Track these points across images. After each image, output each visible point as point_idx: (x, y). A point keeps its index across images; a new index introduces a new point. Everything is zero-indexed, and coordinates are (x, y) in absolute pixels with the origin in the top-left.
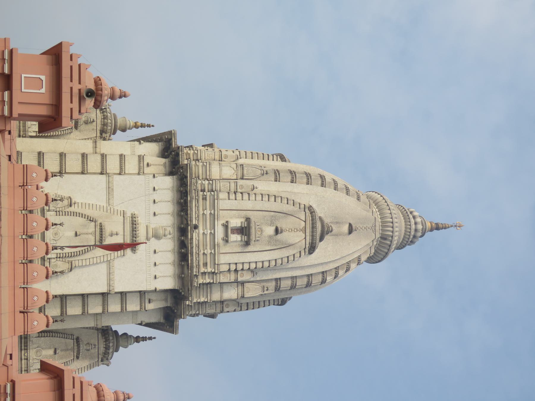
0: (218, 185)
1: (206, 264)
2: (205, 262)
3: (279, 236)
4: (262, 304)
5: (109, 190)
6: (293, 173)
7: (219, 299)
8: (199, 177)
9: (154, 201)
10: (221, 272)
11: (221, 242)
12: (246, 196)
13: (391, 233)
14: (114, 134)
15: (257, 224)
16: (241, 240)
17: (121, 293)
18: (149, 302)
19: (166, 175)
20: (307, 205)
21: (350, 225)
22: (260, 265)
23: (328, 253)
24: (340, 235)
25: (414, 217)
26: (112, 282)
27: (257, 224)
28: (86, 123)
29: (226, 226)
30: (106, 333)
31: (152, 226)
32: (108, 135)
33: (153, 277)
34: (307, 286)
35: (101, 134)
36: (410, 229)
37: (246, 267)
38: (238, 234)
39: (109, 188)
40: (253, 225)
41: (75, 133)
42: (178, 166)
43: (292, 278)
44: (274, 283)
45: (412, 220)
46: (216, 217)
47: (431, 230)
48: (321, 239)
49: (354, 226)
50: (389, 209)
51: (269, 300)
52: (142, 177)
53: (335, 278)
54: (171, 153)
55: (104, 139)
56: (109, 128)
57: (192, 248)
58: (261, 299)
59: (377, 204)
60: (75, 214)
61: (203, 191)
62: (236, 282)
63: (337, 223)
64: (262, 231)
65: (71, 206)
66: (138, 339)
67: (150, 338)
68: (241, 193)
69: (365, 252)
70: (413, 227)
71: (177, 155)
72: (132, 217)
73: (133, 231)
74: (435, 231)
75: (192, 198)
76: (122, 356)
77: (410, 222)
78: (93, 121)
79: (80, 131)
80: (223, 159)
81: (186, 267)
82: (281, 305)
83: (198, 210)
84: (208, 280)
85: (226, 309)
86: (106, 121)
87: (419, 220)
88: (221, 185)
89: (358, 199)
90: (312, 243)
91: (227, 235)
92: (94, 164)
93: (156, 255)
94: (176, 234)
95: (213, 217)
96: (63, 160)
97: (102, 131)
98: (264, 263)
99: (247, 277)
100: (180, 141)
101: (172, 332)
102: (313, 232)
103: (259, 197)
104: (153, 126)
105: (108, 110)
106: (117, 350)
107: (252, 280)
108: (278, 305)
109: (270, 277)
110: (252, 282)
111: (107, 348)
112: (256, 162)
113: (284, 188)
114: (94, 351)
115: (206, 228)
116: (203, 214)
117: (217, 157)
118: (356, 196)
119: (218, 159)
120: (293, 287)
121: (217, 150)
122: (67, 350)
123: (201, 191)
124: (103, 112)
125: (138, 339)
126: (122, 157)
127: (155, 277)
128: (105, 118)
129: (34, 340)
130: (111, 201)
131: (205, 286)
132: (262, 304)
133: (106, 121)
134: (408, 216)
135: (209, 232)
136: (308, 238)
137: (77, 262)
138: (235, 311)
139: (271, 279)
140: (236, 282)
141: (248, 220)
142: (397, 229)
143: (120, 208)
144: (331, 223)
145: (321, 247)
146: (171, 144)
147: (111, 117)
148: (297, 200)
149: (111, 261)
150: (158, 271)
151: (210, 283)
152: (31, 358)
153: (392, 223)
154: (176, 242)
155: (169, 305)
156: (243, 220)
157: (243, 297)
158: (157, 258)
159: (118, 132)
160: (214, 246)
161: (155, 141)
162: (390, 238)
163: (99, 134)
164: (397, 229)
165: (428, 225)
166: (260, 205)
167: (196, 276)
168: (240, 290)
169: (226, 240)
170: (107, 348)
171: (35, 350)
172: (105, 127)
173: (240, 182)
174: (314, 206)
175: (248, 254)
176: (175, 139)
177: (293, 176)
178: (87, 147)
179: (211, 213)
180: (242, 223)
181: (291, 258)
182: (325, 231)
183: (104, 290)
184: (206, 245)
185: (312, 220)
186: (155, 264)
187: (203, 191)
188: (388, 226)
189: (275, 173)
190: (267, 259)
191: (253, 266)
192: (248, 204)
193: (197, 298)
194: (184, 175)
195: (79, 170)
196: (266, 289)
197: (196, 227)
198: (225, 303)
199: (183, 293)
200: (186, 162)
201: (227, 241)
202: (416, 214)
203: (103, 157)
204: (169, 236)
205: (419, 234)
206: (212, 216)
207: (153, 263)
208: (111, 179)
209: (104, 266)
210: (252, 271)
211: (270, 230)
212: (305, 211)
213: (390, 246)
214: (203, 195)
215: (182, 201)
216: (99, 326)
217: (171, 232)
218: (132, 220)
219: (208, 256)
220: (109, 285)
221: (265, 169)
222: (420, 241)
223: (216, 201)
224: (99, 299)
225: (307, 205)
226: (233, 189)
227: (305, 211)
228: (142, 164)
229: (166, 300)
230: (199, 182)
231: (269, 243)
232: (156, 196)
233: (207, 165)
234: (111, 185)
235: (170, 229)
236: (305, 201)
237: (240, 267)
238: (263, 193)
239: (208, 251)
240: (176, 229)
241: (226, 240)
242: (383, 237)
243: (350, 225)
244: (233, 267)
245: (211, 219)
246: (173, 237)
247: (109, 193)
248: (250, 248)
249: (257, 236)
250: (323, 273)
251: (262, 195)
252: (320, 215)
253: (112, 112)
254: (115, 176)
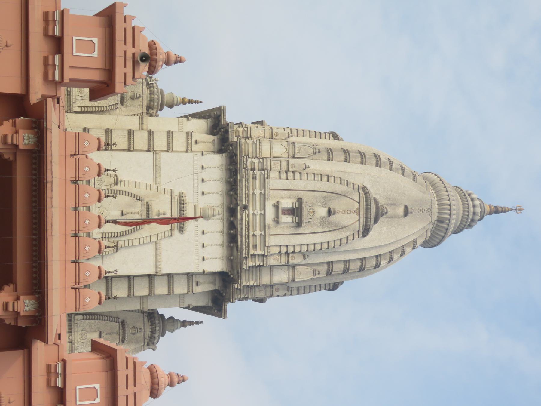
0: (269, 164)
1: (256, 245)
2: (255, 243)
3: (332, 218)
4: (313, 288)
5: (157, 167)
6: (346, 152)
7: (269, 283)
8: (248, 155)
9: (203, 180)
10: (271, 255)
11: (272, 223)
12: (297, 176)
13: (448, 216)
14: (161, 110)
15: (309, 205)
16: (293, 222)
17: (168, 275)
18: (197, 285)
19: (214, 152)
20: (361, 186)
21: (406, 207)
22: (311, 248)
23: (382, 235)
24: (396, 217)
25: (472, 200)
26: (158, 264)
27: (309, 205)
28: (132, 98)
29: (277, 206)
30: (152, 316)
31: (201, 206)
32: (155, 111)
33: (201, 259)
34: (360, 271)
35: (148, 110)
36: (468, 212)
37: (297, 249)
38: (289, 215)
39: (156, 165)
40: (304, 206)
41: (121, 109)
42: (227, 143)
43: (345, 261)
44: (325, 267)
45: (471, 203)
46: (266, 197)
47: (490, 214)
48: (376, 221)
49: (409, 208)
50: (447, 191)
51: (321, 285)
52: (190, 155)
53: (389, 262)
54: (220, 129)
55: (151, 115)
56: (156, 104)
57: (242, 229)
58: (312, 284)
59: (433, 185)
60: (122, 193)
61: (253, 169)
62: (287, 265)
63: (392, 204)
64: (314, 212)
65: (117, 184)
66: (184, 324)
67: (197, 323)
68: (293, 172)
69: (421, 236)
70: (471, 210)
71: (227, 132)
72: (180, 197)
73: (180, 211)
74: (494, 214)
75: (241, 177)
76: (167, 341)
77: (468, 205)
78: (140, 97)
79: (126, 107)
80: (274, 137)
81: (235, 249)
82: (332, 290)
83: (248, 189)
84: (257, 263)
85: (276, 294)
86: (153, 96)
87: (477, 203)
88: (272, 164)
89: (414, 179)
90: (366, 225)
91: (277, 216)
92: (141, 140)
93: (205, 235)
94: (225, 214)
95: (264, 197)
96: (109, 137)
97: (149, 108)
98: (316, 246)
99: (297, 260)
100: (230, 118)
101: (221, 316)
102: (367, 214)
103: (311, 177)
104: (201, 102)
105: (155, 85)
106: (163, 334)
107: (303, 263)
108: (330, 290)
109: (322, 261)
110: (304, 265)
111: (153, 332)
112: (307, 140)
113: (337, 167)
114: (140, 335)
115: (256, 209)
116: (253, 193)
117: (268, 135)
118: (412, 177)
119: (268, 137)
120: (346, 271)
121: (267, 128)
122: (111, 333)
123: (251, 170)
124: (150, 88)
125: (184, 324)
126: (169, 134)
127: (204, 259)
128: (152, 93)
129: (79, 322)
130: (158, 180)
131: (254, 269)
132: (313, 288)
133: (153, 96)
134: (466, 198)
135: (259, 212)
136: (362, 220)
137: (123, 243)
138: (285, 295)
139: (323, 263)
140: (287, 265)
141: (300, 200)
142: (454, 212)
143: (168, 187)
144: (387, 204)
145: (375, 229)
146: (220, 121)
147: (158, 92)
148: (351, 181)
149: (158, 242)
150: (206, 253)
151: (259, 266)
152: (76, 341)
153: (450, 205)
154: (225, 222)
155: (217, 288)
156: (295, 200)
157: (293, 281)
158: (205, 239)
159: (165, 108)
160: (264, 227)
161: (204, 118)
162: (447, 221)
163: (145, 110)
164: (454, 212)
165: (487, 208)
166: (312, 185)
167: (246, 258)
168: (291, 274)
169: (277, 221)
170: (153, 332)
171: (79, 333)
172: (152, 103)
173: (292, 161)
174: (368, 187)
175: (299, 236)
176: (225, 115)
177: (347, 155)
178: (133, 123)
179: (261, 193)
180: (293, 203)
181: (344, 241)
182: (380, 213)
183: (151, 271)
184: (256, 226)
185: (367, 201)
186: (203, 246)
187: (253, 169)
188: (445, 209)
189: (328, 151)
190: (319, 241)
191: (304, 248)
192: (299, 184)
193: (247, 280)
194: (233, 152)
195: (126, 147)
196: (317, 272)
197: (246, 207)
198: (275, 287)
199: (232, 276)
200: (235, 139)
201: (278, 222)
202: (474, 196)
203: (150, 133)
204: (218, 217)
205: (478, 217)
206: (262, 196)
208: (158, 157)
209: (151, 247)
210: (303, 254)
211: (322, 212)
212: (359, 192)
213: (447, 229)
214: (254, 174)
215: (232, 180)
216: (146, 309)
217: (220, 212)
218: (180, 200)
219: (258, 237)
220: (156, 267)
221: (317, 148)
222: (478, 226)
223: (267, 180)
224: (146, 281)
225: (361, 186)
226: (284, 168)
227: (359, 192)
228: (190, 141)
229: (214, 283)
230: (249, 160)
231: (321, 224)
232: (205, 175)
233: (257, 143)
234: (158, 163)
235: (218, 209)
236: (359, 181)
237: (291, 249)
238: (315, 172)
239: (258, 233)
240: (225, 209)
241: (277, 221)
242: (440, 221)
243: (406, 207)
244: (284, 250)
245: (262, 199)
246: (222, 218)
247: (156, 171)
248: (301, 230)
249: (309, 217)
250: (377, 256)
251: (314, 174)
252: (374, 196)
253: (159, 88)
254: (162, 154)
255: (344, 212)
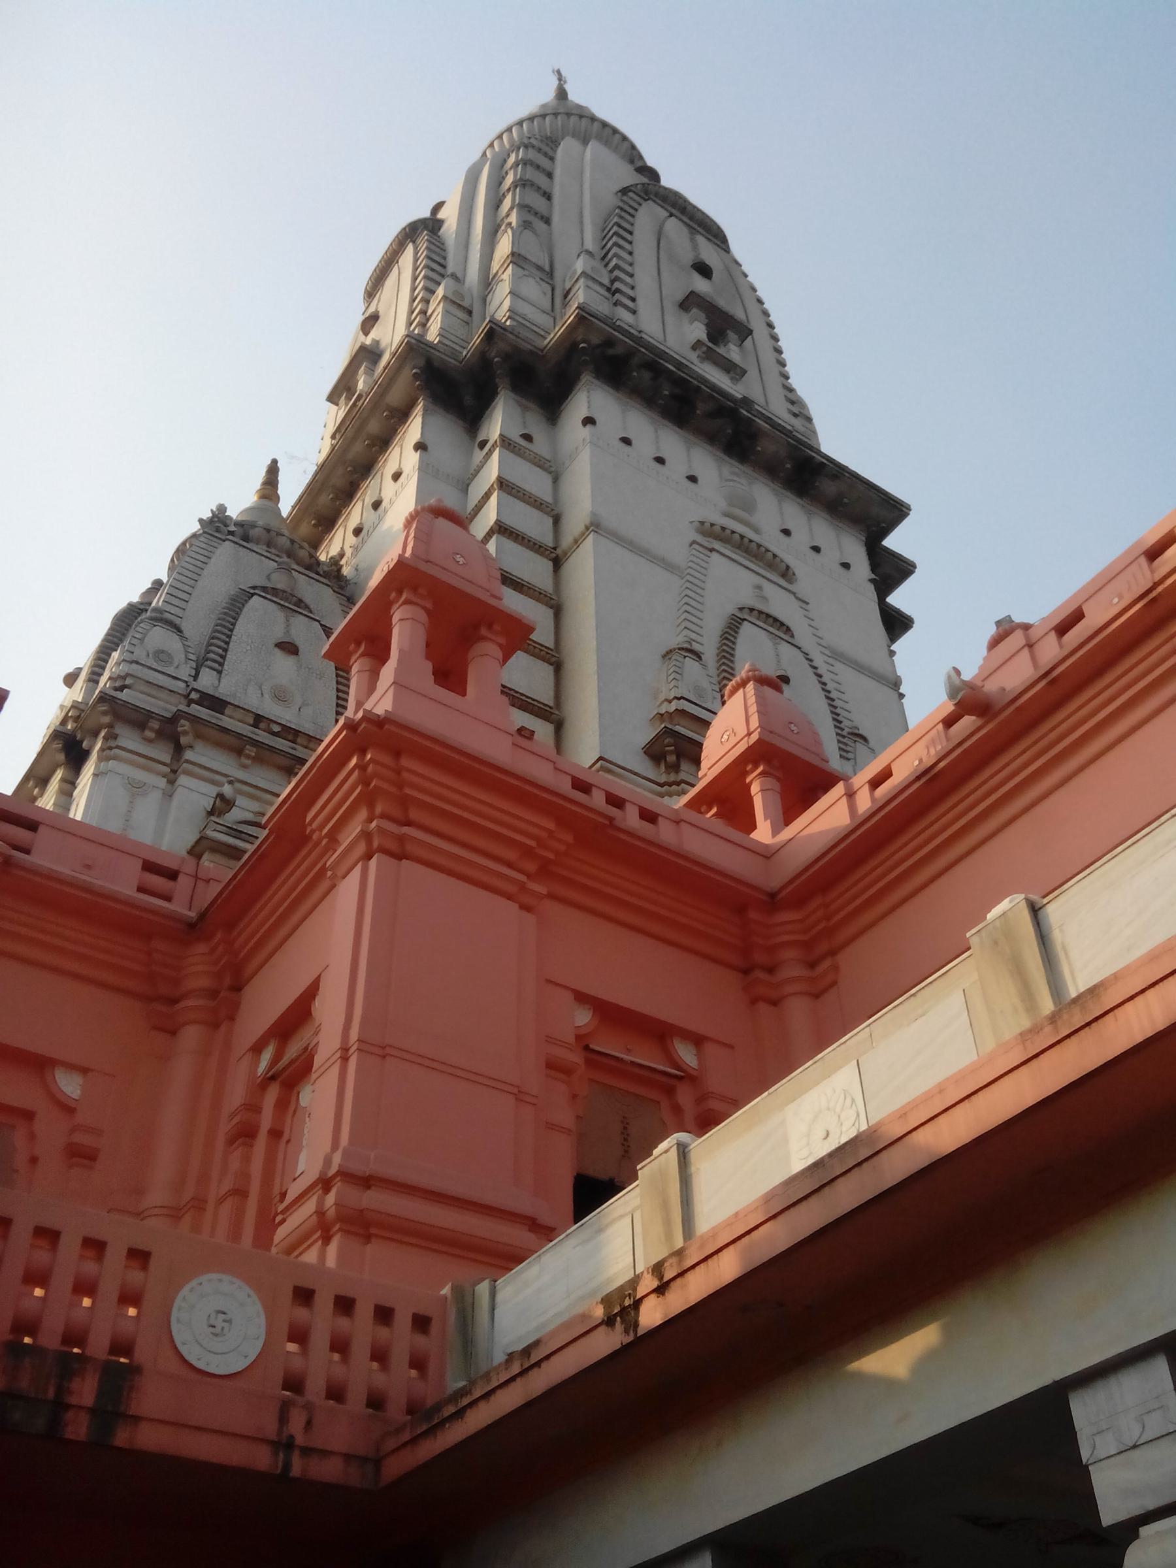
31: (723, 504)
80: (466, 304)
117: (462, 315)
156: (685, 317)
207: (813, 554)
211: (701, 285)
255: (695, 247)
